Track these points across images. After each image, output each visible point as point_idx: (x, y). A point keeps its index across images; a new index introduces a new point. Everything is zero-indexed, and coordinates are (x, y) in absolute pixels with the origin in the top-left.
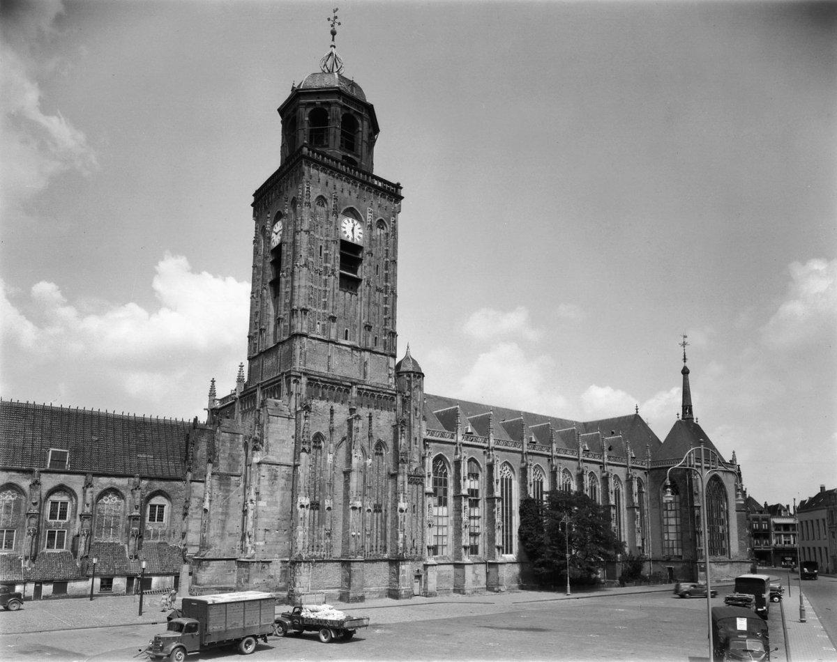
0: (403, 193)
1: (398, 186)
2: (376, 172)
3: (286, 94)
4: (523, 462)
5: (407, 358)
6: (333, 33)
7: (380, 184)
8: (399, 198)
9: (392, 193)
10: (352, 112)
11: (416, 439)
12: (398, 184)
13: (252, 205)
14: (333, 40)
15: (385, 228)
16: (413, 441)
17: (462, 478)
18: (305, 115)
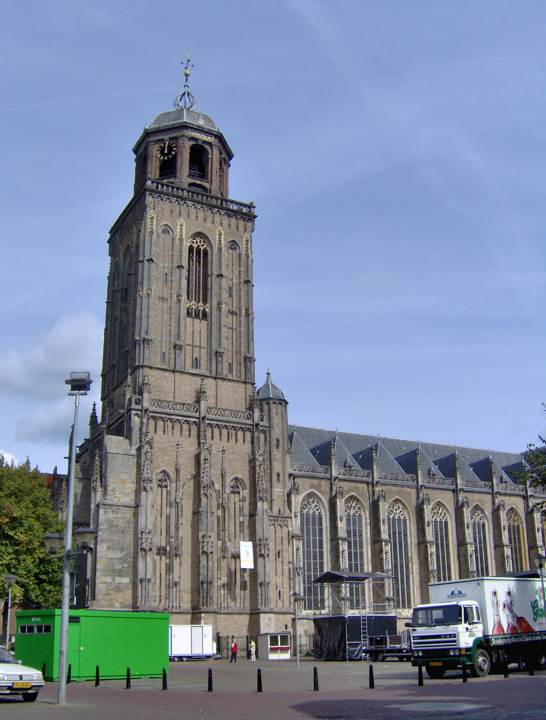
0: (256, 212)
1: (250, 206)
2: (230, 197)
3: (139, 134)
5: (266, 386)
8: (251, 218)
9: (246, 214)
10: (200, 143)
11: (278, 475)
12: (252, 204)
14: (187, 81)
16: (275, 477)
18: (155, 152)
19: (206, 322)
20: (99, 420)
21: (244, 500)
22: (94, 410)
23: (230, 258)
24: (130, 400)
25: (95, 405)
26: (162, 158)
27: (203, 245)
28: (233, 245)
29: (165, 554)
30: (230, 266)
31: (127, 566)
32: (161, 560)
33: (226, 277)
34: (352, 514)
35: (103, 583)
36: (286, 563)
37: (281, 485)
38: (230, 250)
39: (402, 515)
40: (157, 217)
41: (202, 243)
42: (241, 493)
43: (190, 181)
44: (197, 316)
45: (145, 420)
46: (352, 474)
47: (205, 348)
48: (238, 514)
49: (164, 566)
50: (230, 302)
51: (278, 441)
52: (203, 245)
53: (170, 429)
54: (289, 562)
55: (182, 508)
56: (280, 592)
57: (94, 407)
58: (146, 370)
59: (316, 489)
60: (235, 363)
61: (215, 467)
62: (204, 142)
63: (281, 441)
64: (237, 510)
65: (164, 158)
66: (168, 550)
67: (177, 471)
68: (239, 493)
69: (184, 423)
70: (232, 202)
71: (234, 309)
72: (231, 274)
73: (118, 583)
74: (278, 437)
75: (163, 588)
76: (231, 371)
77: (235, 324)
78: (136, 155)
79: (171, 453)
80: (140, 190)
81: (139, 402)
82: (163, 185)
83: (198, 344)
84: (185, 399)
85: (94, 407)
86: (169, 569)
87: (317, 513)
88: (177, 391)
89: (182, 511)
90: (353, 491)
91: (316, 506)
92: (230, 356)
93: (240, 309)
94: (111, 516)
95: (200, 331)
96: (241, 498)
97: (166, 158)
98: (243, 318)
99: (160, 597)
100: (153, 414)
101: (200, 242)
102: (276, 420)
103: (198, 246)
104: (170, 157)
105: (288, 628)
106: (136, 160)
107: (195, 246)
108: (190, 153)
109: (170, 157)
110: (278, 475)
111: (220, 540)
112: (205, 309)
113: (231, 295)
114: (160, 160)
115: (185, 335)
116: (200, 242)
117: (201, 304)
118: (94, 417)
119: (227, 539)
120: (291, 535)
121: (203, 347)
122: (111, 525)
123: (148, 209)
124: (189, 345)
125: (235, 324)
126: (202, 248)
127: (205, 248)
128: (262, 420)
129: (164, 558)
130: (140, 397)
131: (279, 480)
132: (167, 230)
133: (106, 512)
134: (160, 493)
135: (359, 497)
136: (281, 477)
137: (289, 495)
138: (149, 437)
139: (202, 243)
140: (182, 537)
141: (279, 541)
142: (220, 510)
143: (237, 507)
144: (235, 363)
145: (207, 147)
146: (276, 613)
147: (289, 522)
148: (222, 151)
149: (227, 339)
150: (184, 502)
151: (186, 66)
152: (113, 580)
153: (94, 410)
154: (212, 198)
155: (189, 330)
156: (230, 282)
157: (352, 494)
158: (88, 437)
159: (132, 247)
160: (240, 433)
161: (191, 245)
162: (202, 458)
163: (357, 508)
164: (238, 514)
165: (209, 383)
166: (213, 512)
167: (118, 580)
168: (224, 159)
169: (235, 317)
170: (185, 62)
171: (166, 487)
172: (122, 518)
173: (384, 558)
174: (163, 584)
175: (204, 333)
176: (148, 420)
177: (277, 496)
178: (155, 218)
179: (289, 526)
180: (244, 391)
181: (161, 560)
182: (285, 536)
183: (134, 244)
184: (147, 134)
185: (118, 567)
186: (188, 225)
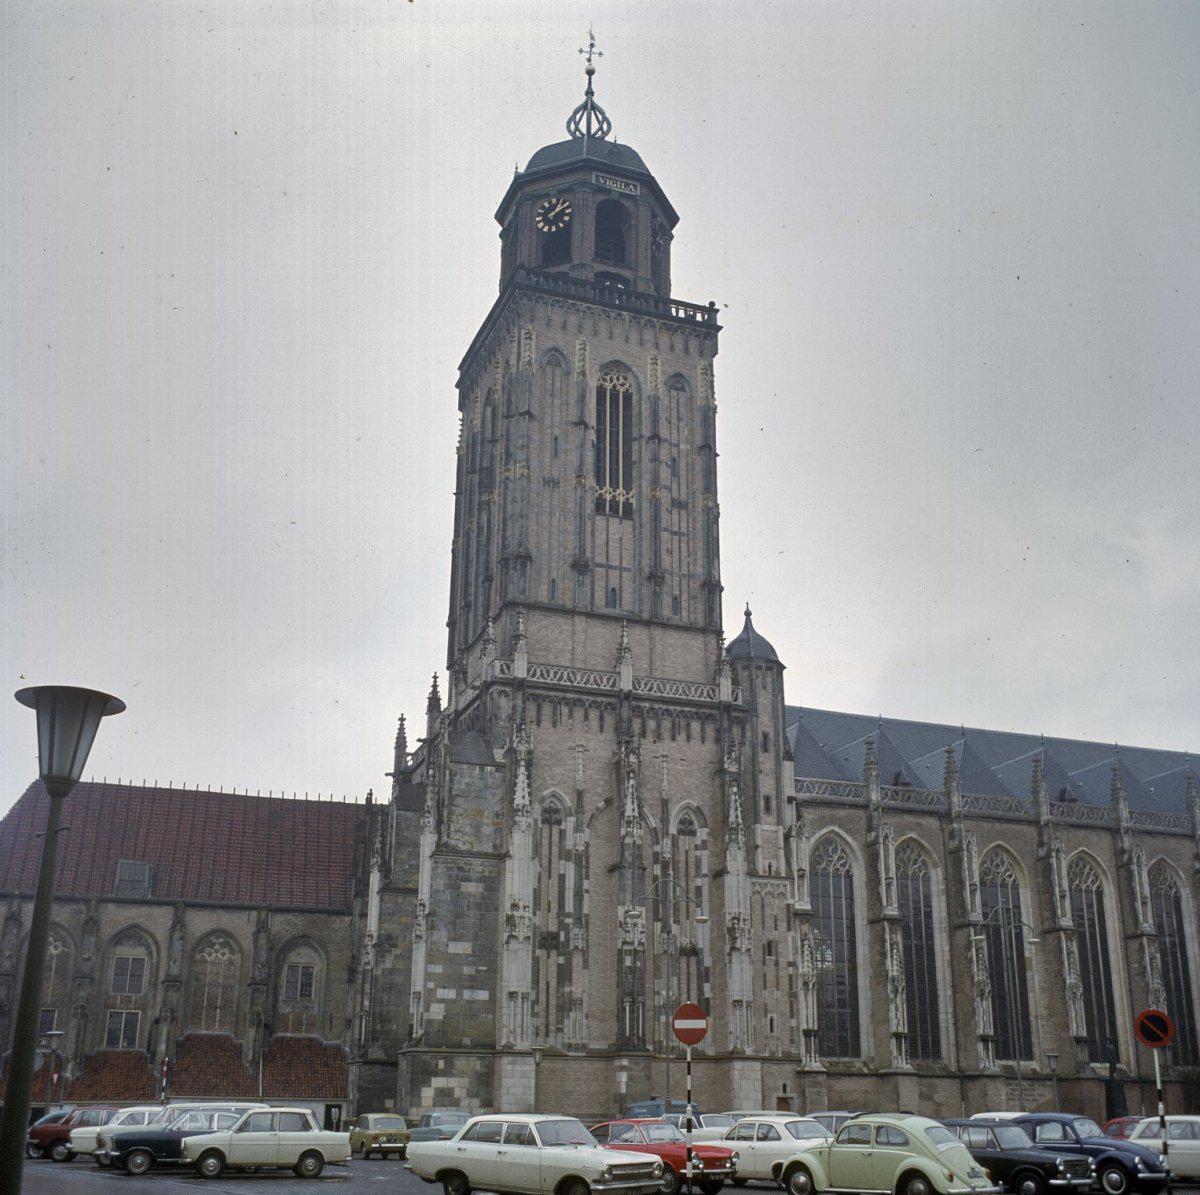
1: (711, 310)
2: (673, 296)
4: (1041, 844)
6: (590, 73)
7: (682, 314)
9: (702, 328)
10: (615, 196)
11: (767, 799)
15: (687, 388)
17: (883, 882)
19: (630, 522)
20: (444, 704)
21: (704, 846)
22: (435, 686)
23: (674, 405)
25: (435, 677)
28: (677, 382)
29: (557, 947)
30: (674, 421)
31: (485, 968)
32: (548, 957)
33: (666, 440)
34: (910, 873)
35: (442, 1001)
36: (783, 961)
37: (771, 819)
38: (674, 393)
39: (1010, 876)
41: (622, 381)
42: (698, 834)
43: (599, 268)
45: (519, 702)
46: (909, 798)
47: (629, 570)
48: (692, 872)
49: (553, 969)
50: (675, 486)
52: (622, 385)
53: (565, 718)
54: (792, 964)
55: (587, 862)
56: (771, 1020)
57: (435, 682)
59: (840, 826)
61: (649, 786)
62: (622, 195)
63: (771, 736)
64: (692, 866)
66: (562, 938)
67: (580, 794)
68: (693, 833)
69: (590, 706)
70: (679, 304)
72: (675, 436)
73: (468, 1001)
74: (766, 729)
75: (553, 1010)
76: (676, 609)
78: (502, 225)
79: (568, 762)
82: (547, 278)
83: (617, 563)
84: (593, 662)
85: (435, 682)
86: (564, 974)
87: (843, 871)
88: (579, 649)
89: (587, 867)
90: (912, 830)
91: (840, 858)
92: (676, 584)
95: (621, 539)
96: (699, 843)
97: (554, 229)
99: (547, 1026)
101: (618, 379)
102: (764, 700)
103: (614, 386)
104: (561, 225)
105: (788, 1090)
106: (501, 235)
107: (609, 386)
109: (561, 225)
110: (767, 799)
111: (660, 920)
112: (628, 499)
113: (675, 474)
115: (593, 547)
116: (618, 379)
118: (434, 699)
119: (672, 919)
120: (792, 911)
121: (625, 569)
126: (622, 390)
127: (627, 390)
129: (554, 953)
131: (768, 809)
134: (545, 835)
136: (774, 804)
139: (622, 381)
140: (587, 915)
141: (770, 923)
142: (659, 866)
143: (692, 859)
144: (685, 597)
145: (627, 203)
146: (764, 1060)
148: (658, 211)
149: (670, 552)
150: (592, 850)
151: (588, 56)
152: (459, 994)
153: (435, 686)
155: (600, 539)
157: (909, 836)
158: (424, 736)
160: (695, 726)
161: (601, 386)
163: (919, 864)
164: (692, 872)
165: (636, 637)
166: (644, 869)
167: (467, 994)
168: (661, 225)
169: (683, 512)
170: (587, 48)
171: (559, 823)
173: (975, 958)
174: (553, 1002)
175: (628, 542)
176: (524, 702)
177: (766, 841)
178: (533, 337)
179: (788, 895)
180: (702, 646)
181: (548, 957)
182: (782, 915)
185: (467, 970)
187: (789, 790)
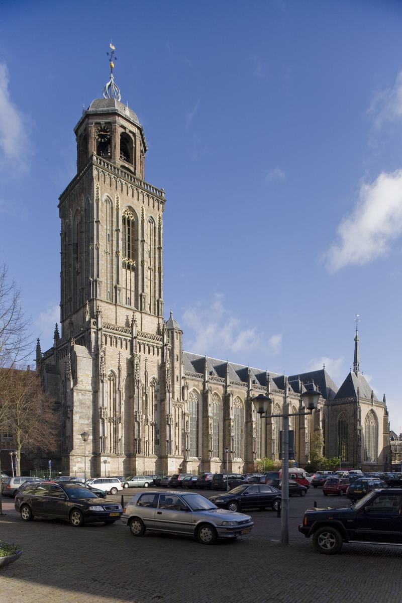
10: (127, 131)
13: (59, 199)
18: (94, 132)
24: (89, 321)
26: (100, 140)
27: (131, 217)
40: (101, 188)
41: (131, 215)
44: (129, 268)
50: (149, 261)
51: (177, 357)
52: (131, 217)
58: (99, 303)
60: (152, 304)
62: (130, 131)
65: (101, 140)
71: (152, 267)
75: (112, 442)
77: (152, 277)
80: (84, 163)
81: (96, 324)
93: (155, 267)
94: (81, 397)
97: (103, 141)
98: (157, 274)
100: (105, 333)
103: (128, 217)
108: (121, 139)
113: (150, 257)
114: (97, 141)
117: (131, 260)
122: (82, 403)
123: (95, 180)
124: (124, 288)
125: (152, 277)
126: (132, 219)
128: (169, 342)
130: (95, 320)
132: (109, 201)
133: (78, 395)
135: (218, 394)
137: (183, 388)
138: (103, 347)
139: (131, 215)
145: (131, 135)
147: (183, 406)
154: (137, 180)
156: (149, 247)
159: (81, 210)
161: (124, 216)
162: (135, 363)
165: (138, 315)
172: (88, 399)
183: (83, 209)
184: (88, 116)
186: (122, 199)
187: (183, 375)
